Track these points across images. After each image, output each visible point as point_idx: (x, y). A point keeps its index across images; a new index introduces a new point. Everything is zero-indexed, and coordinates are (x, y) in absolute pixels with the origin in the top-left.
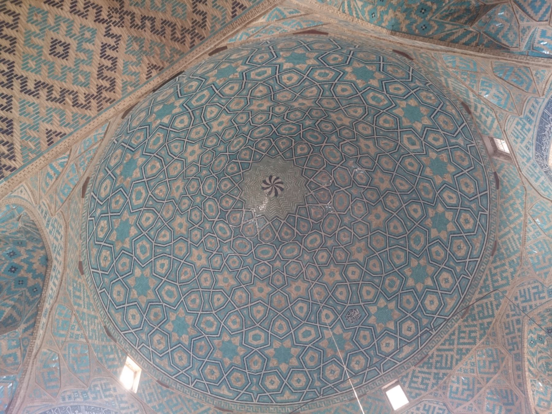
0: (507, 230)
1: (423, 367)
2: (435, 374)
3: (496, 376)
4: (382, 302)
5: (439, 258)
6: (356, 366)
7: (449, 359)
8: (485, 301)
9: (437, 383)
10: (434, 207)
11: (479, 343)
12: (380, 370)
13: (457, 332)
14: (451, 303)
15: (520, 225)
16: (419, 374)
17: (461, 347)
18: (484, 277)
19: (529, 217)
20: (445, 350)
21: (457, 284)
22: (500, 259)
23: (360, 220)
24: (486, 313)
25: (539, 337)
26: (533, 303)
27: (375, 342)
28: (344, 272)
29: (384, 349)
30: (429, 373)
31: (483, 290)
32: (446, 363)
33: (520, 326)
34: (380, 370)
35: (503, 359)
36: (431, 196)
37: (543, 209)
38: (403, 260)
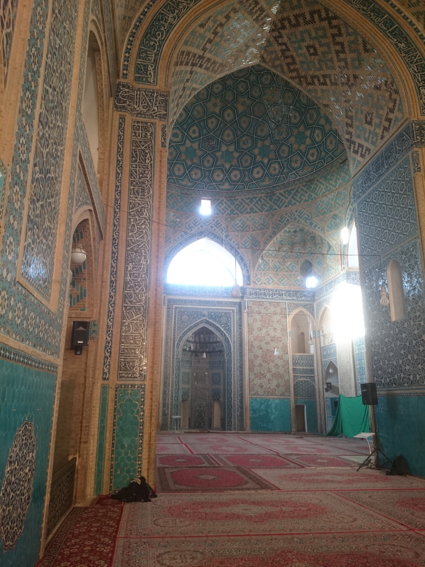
0: (324, 183)
1: (229, 201)
2: (232, 209)
3: (258, 231)
4: (232, 148)
5: (282, 155)
6: (194, 175)
7: (244, 208)
8: (283, 198)
9: (230, 215)
10: (306, 129)
11: (263, 213)
12: (206, 187)
13: (257, 199)
14: (267, 182)
15: (330, 188)
16: (224, 204)
17: (254, 207)
18: (293, 187)
19: (337, 191)
20: (245, 202)
21: (278, 177)
22: (307, 188)
23: (261, 86)
24: (278, 203)
25: (290, 231)
26: (301, 220)
27: (213, 169)
28: (223, 110)
29: (215, 176)
30: (230, 207)
31: (287, 193)
32: (241, 209)
33: (287, 223)
34: (206, 187)
35: (268, 228)
36: (311, 122)
37: (344, 196)
38: (263, 135)
